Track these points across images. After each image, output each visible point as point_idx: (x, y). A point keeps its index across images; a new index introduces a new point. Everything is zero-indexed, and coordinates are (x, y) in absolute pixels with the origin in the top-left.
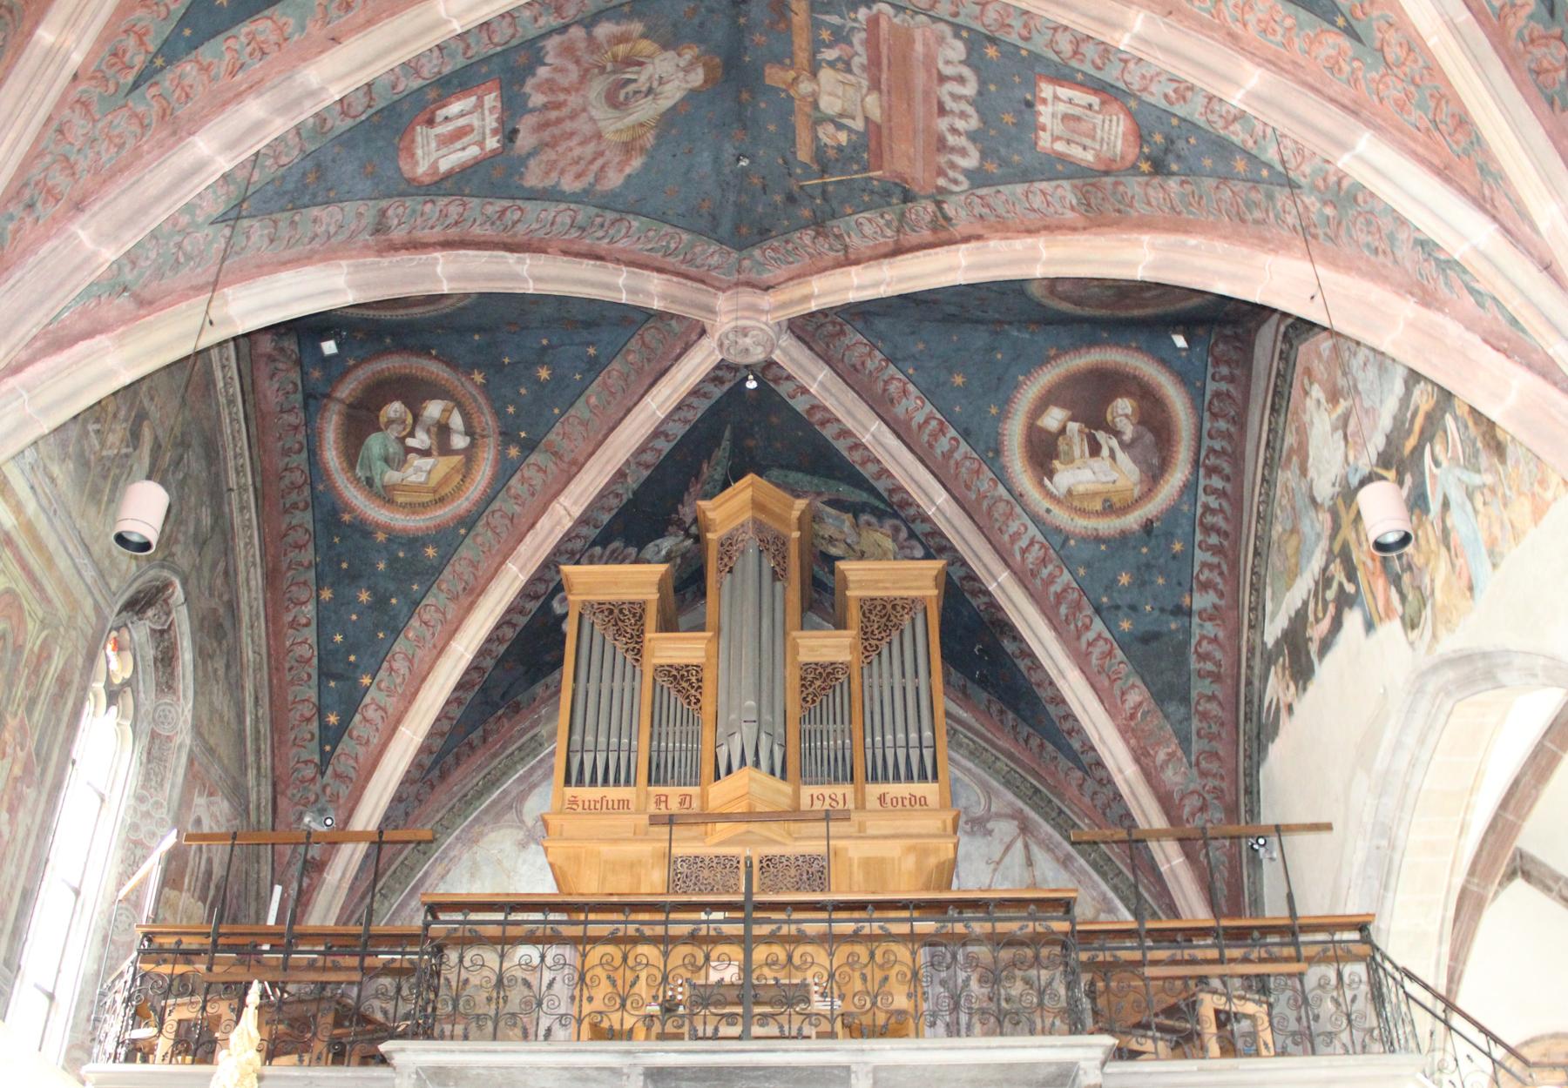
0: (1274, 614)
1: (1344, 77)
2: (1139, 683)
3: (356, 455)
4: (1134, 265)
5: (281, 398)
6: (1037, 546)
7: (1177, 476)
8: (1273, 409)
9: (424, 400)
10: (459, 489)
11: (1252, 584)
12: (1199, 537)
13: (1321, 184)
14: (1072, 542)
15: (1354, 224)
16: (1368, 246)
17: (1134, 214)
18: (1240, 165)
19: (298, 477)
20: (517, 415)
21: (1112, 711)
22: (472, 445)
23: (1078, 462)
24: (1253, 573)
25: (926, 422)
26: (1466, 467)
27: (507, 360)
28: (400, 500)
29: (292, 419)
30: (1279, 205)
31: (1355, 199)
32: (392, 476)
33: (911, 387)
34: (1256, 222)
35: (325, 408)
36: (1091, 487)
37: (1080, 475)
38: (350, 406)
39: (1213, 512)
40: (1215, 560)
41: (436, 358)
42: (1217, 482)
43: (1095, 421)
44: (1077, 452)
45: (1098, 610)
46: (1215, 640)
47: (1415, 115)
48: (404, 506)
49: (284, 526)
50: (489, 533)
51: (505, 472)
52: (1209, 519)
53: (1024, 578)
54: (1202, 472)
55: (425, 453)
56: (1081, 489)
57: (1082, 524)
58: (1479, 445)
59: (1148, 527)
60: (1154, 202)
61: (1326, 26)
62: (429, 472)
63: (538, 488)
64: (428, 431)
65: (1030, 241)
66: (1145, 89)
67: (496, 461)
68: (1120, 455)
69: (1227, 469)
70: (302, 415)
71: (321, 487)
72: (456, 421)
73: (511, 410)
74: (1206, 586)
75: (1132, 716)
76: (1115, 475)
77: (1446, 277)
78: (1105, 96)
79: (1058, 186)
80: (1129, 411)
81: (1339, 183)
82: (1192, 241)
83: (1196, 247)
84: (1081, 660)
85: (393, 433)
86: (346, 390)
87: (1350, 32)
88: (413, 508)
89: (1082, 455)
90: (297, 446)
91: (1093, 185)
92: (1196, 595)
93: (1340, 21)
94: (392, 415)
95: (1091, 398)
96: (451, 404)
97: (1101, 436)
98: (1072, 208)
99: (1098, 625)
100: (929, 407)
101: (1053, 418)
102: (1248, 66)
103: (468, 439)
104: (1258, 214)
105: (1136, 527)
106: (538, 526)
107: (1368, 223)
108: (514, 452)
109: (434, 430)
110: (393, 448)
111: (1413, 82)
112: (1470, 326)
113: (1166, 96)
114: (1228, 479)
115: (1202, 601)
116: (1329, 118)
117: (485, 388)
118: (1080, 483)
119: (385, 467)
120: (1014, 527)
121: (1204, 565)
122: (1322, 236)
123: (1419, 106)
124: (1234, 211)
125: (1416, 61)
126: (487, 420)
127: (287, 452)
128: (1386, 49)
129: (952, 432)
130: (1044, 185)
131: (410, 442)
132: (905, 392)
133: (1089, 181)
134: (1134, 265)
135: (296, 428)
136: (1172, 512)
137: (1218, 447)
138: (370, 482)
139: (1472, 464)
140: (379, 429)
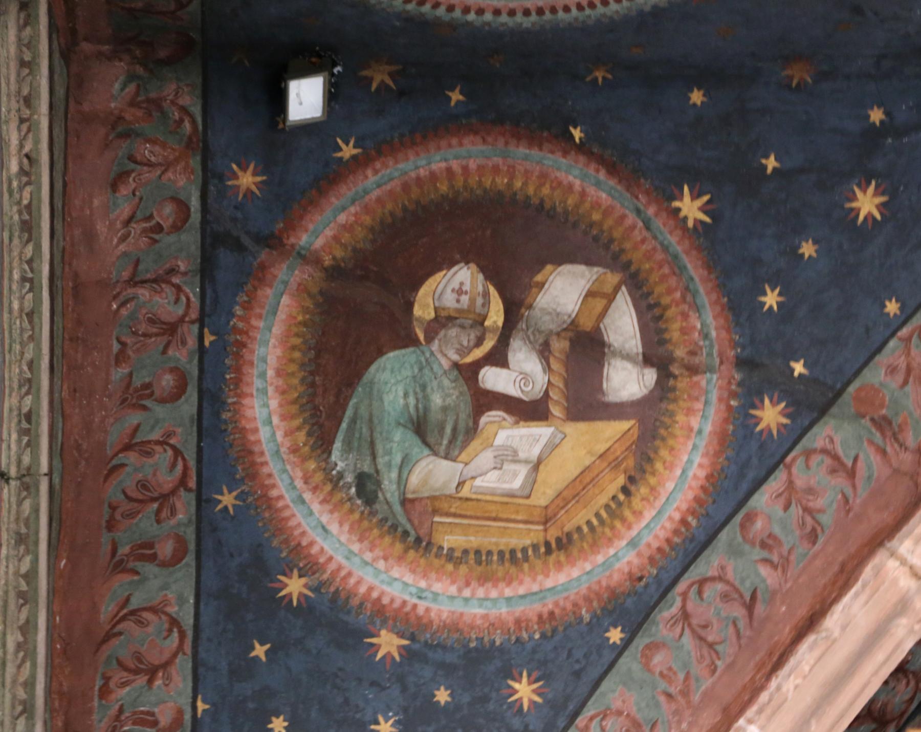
3: (340, 406)
5: (137, 241)
9: (541, 264)
10: (615, 510)
19: (161, 470)
20: (786, 311)
22: (663, 390)
27: (771, 163)
28: (449, 540)
29: (165, 305)
32: (433, 473)
35: (259, 276)
38: (335, 272)
41: (581, 148)
48: (455, 558)
49: (107, 609)
50: (687, 640)
51: (745, 466)
55: (529, 411)
62: (537, 466)
63: (826, 519)
64: (544, 352)
67: (722, 438)
70: (193, 292)
71: (227, 499)
72: (623, 325)
73: (771, 299)
85: (447, 351)
86: (329, 227)
88: (483, 564)
90: (168, 381)
94: (449, 301)
96: (613, 278)
103: (651, 376)
106: (833, 621)
108: (771, 415)
109: (559, 346)
110: (444, 395)
117: (705, 237)
119: (418, 449)
126: (704, 325)
127: (137, 396)
131: (494, 379)
135: (171, 329)
138: (367, 487)
140: (410, 341)
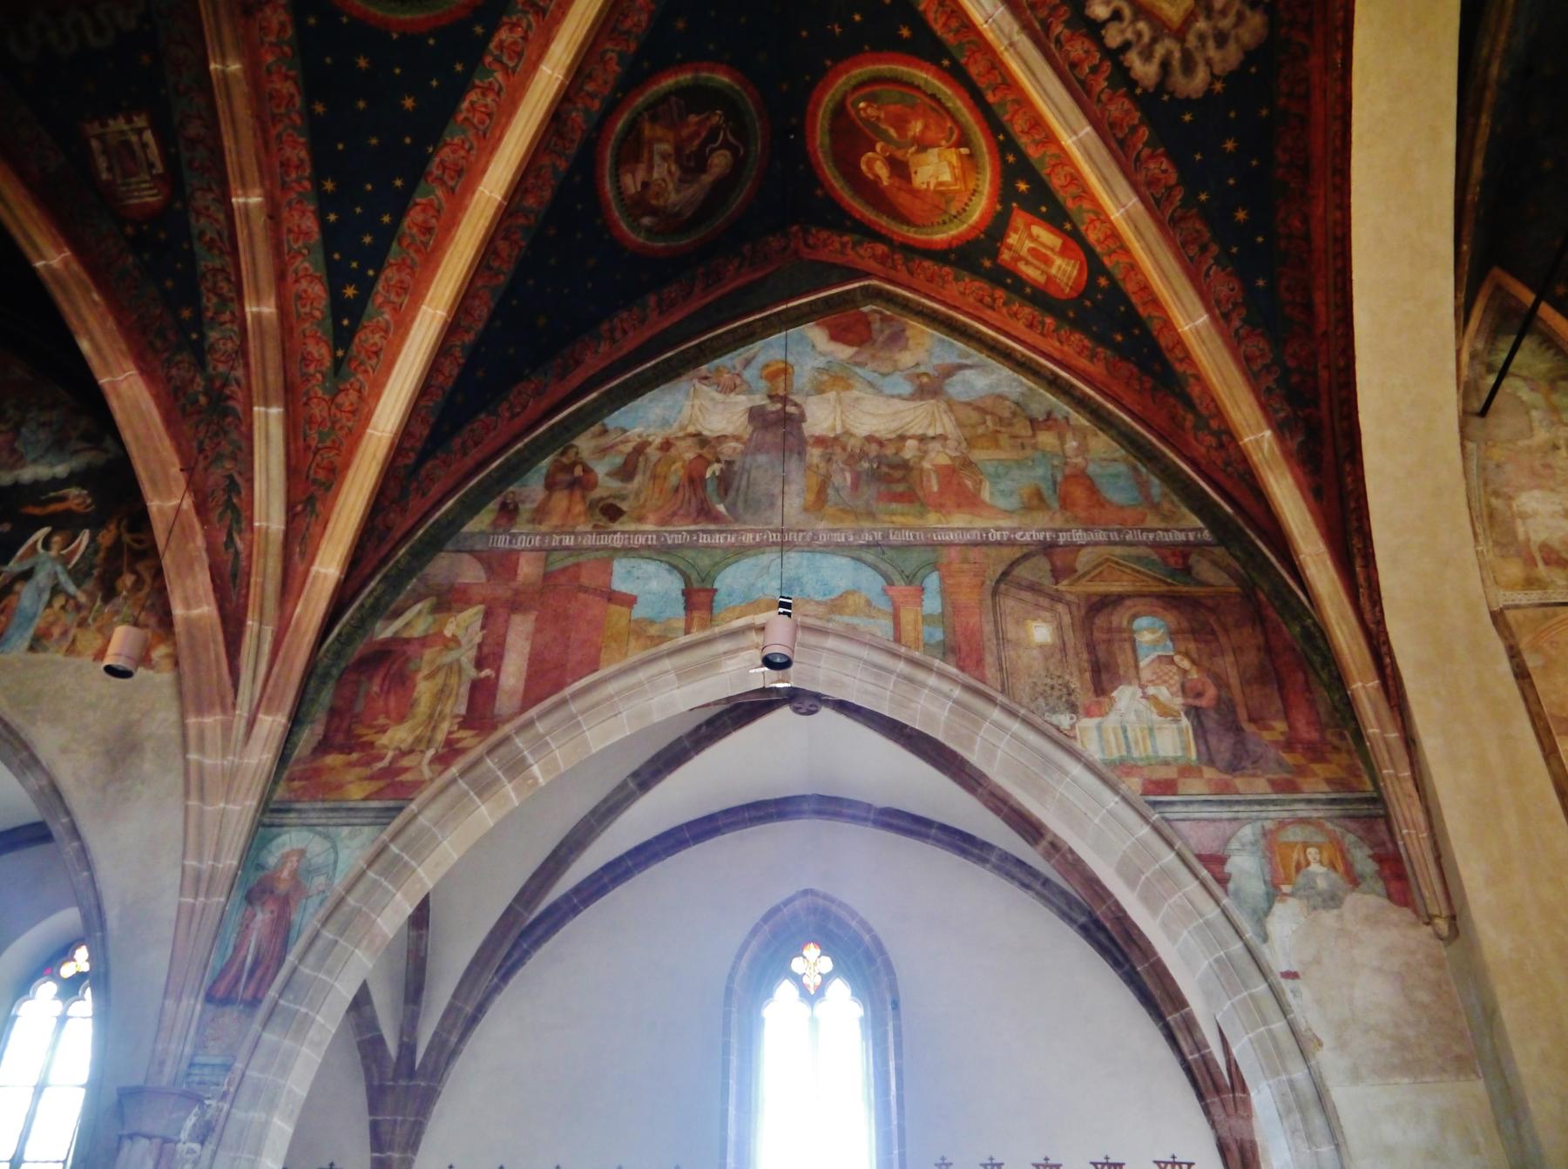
4: (42, 257)
13: (218, 384)
18: (186, 314)
30: (178, 358)
31: (226, 416)
66: (198, 213)
77: (224, 512)
81: (229, 397)
82: (96, 297)
83: (94, 301)
87: (338, 364)
93: (340, 353)
102: (273, 301)
104: (158, 343)
111: (334, 423)
112: (211, 549)
113: (202, 233)
116: (274, 378)
123: (320, 433)
128: (342, 395)
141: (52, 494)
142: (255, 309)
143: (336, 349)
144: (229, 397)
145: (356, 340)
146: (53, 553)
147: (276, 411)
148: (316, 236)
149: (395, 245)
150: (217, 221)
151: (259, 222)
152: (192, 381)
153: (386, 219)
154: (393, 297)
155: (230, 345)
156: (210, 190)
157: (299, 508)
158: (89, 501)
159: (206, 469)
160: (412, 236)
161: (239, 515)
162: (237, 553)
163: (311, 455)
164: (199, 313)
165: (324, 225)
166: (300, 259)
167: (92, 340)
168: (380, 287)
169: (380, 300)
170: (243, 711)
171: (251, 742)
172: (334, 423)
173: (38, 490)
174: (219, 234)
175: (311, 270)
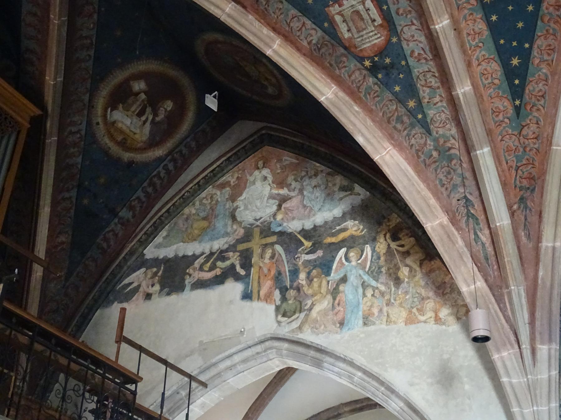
0: (158, 246)
1: (496, 119)
2: (70, 233)
4: (323, 94)
6: (78, 135)
7: (159, 152)
8: (228, 159)
11: (155, 223)
12: (145, 184)
13: (441, 141)
14: (95, 146)
15: (442, 168)
16: (441, 180)
17: (337, 72)
18: (412, 104)
21: (50, 237)
23: (130, 113)
24: (159, 218)
25: (86, 38)
26: (368, 273)
30: (413, 132)
31: (451, 160)
33: (95, 16)
34: (395, 128)
36: (124, 128)
37: (123, 119)
39: (160, 178)
40: (144, 199)
42: (171, 166)
43: (153, 102)
44: (133, 109)
45: (79, 186)
46: (116, 235)
47: (512, 158)
52: (155, 179)
53: (61, 145)
54: (169, 158)
56: (120, 125)
57: (107, 141)
58: (383, 270)
59: (131, 163)
60: (353, 77)
61: (510, 97)
65: (272, 34)
66: (408, 41)
68: (148, 125)
69: (179, 165)
74: (131, 208)
75: (56, 247)
76: (138, 131)
77: (468, 219)
78: (385, 24)
79: (315, 29)
80: (169, 109)
81: (450, 149)
82: (356, 108)
83: (356, 111)
84: (54, 204)
87: (517, 109)
89: (133, 112)
91: (333, 45)
92: (125, 209)
93: (517, 103)
95: (161, 89)
97: (149, 110)
98: (309, 43)
99: (74, 193)
100: (94, 32)
101: (139, 86)
102: (469, 83)
104: (399, 126)
105: (126, 160)
107: (449, 173)
111: (524, 148)
112: (469, 246)
113: (413, 52)
114: (175, 167)
115: (124, 213)
118: (122, 122)
120: (76, 118)
121: (138, 198)
122: (422, 159)
123: (517, 157)
124: (389, 115)
125: (535, 144)
128: (526, 128)
129: (92, 53)
130: (309, 23)
132: (91, 16)
133: (332, 41)
134: (323, 94)
136: (146, 165)
137: (184, 152)
139: (375, 273)
141: (338, 228)
142: (462, 91)
143: (514, 100)
144: (450, 149)
145: (527, 91)
146: (354, 263)
147: (487, 150)
148: (486, 33)
149: (539, 23)
150: (420, 42)
151: (451, 34)
152: (425, 144)
153: (530, 8)
154: (546, 57)
155: (443, 116)
156: (413, 24)
157: (515, 207)
158: (361, 227)
159: (449, 196)
160: (550, 14)
161: (477, 219)
162: (483, 245)
163: (514, 172)
164: (419, 103)
165: (491, 25)
166: (478, 51)
167: (363, 135)
168: (535, 52)
169: (537, 61)
170: (526, 346)
171: (538, 364)
172: (524, 148)
173: (328, 227)
174: (423, 49)
175: (487, 56)
